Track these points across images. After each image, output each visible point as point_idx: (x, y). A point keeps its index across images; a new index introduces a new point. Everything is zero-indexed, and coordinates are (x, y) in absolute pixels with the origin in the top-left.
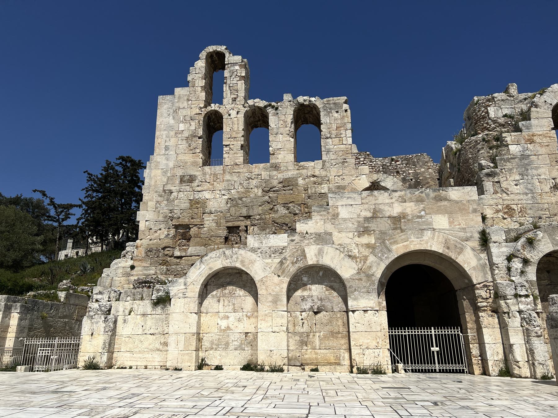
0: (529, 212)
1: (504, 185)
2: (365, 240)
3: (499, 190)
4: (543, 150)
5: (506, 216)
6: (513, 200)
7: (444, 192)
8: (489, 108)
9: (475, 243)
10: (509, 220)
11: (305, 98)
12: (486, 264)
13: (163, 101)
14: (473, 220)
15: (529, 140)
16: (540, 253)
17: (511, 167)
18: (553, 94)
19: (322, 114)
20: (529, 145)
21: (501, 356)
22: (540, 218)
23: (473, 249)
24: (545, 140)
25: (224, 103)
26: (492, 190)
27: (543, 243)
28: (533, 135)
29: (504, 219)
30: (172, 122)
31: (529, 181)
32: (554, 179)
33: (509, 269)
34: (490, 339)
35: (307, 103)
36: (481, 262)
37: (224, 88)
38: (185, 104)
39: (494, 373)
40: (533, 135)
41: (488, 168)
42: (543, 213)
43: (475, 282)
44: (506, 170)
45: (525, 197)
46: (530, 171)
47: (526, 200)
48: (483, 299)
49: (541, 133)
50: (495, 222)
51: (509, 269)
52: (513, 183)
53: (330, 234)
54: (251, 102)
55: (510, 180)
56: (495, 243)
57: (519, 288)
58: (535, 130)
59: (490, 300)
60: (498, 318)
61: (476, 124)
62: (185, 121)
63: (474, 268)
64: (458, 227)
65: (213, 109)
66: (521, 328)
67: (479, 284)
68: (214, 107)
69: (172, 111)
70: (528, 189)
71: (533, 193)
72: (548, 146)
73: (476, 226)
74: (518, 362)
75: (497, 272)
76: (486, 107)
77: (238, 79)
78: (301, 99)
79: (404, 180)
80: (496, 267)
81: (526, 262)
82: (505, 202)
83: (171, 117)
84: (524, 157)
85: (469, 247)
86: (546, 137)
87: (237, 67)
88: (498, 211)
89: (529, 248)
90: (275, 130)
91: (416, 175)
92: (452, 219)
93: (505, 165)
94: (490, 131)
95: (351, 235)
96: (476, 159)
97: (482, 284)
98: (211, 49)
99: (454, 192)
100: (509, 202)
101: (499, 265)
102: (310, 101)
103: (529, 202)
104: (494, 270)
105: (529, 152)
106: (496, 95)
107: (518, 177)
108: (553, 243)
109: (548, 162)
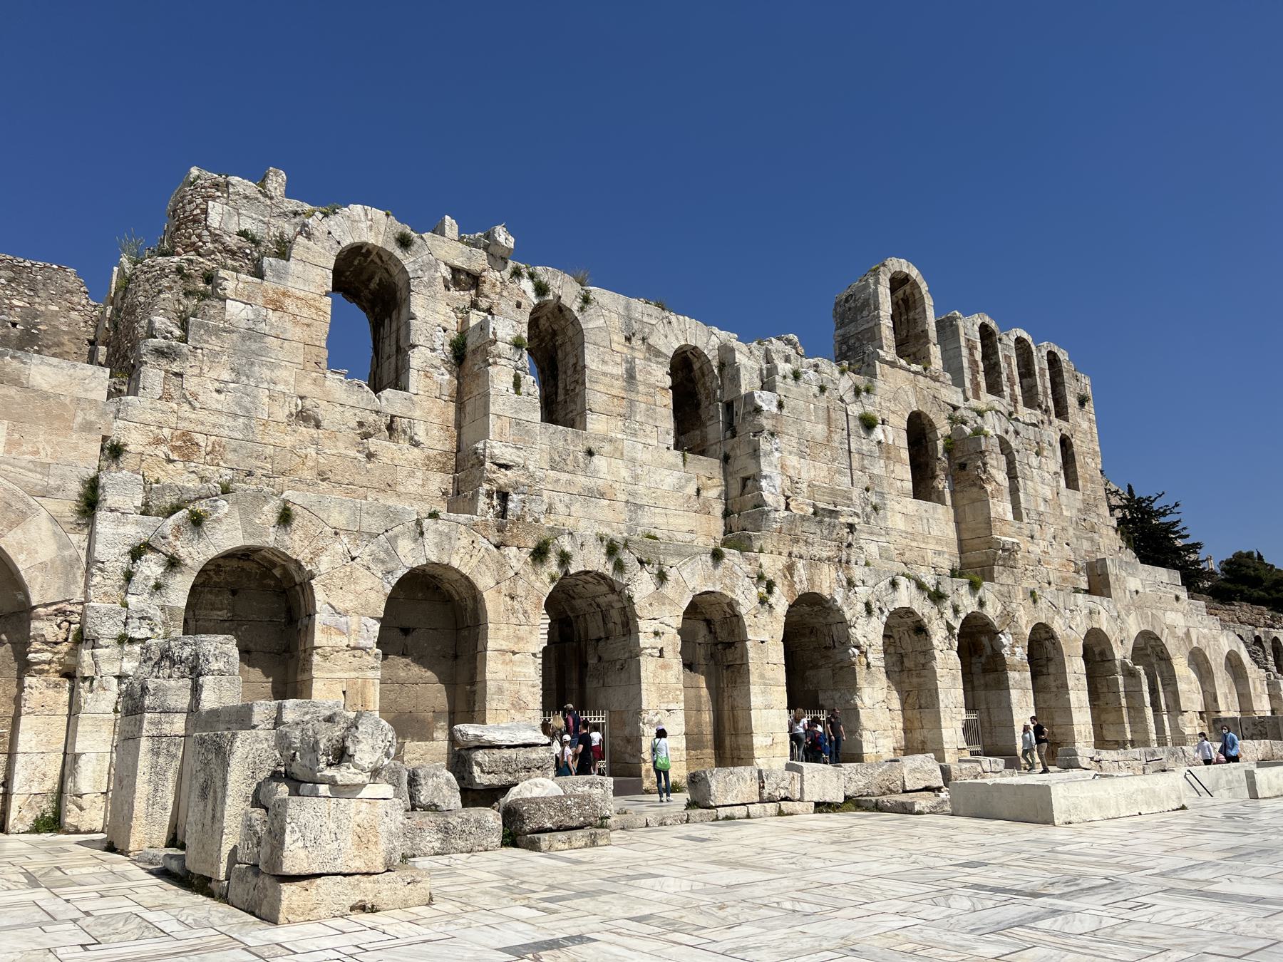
0: (230, 456)
1: (191, 384)
3: (176, 394)
4: (296, 332)
5: (174, 456)
6: (202, 424)
7: (15, 364)
8: (210, 203)
9: (67, 506)
10: (180, 465)
12: (78, 559)
14: (75, 448)
15: (273, 301)
16: (212, 548)
17: (218, 349)
18: (348, 223)
20: (270, 312)
21: (51, 784)
22: (250, 474)
23: (55, 520)
24: (306, 312)
26: (159, 391)
27: (224, 527)
28: (284, 294)
29: (170, 461)
31: (249, 389)
32: (302, 398)
33: (129, 576)
34: (33, 744)
36: (66, 553)
39: (20, 827)
40: (284, 294)
41: (165, 338)
42: (259, 464)
43: (35, 600)
44: (206, 351)
45: (231, 423)
46: (256, 368)
47: (231, 429)
48: (46, 643)
49: (302, 294)
50: (144, 464)
51: (129, 576)
52: (212, 386)
55: (207, 377)
56: (112, 511)
57: (134, 623)
58: (291, 285)
59: (64, 648)
60: (72, 690)
61: (178, 229)
63: (43, 566)
64: (29, 457)
66: (112, 716)
67: (46, 605)
70: (241, 406)
71: (250, 418)
72: (308, 325)
73: (81, 464)
74: (80, 796)
75: (96, 580)
76: (206, 198)
80: (100, 569)
81: (173, 564)
82: (182, 425)
84: (252, 334)
85: (44, 513)
86: (310, 306)
88: (158, 441)
89: (189, 535)
92: (17, 436)
93: (206, 342)
94: (199, 255)
96: (149, 308)
97: (54, 607)
99: (45, 369)
100: (191, 427)
101: (107, 565)
103: (236, 435)
104: (93, 575)
105: (267, 328)
106: (234, 179)
107: (226, 375)
108: (245, 531)
109: (301, 359)
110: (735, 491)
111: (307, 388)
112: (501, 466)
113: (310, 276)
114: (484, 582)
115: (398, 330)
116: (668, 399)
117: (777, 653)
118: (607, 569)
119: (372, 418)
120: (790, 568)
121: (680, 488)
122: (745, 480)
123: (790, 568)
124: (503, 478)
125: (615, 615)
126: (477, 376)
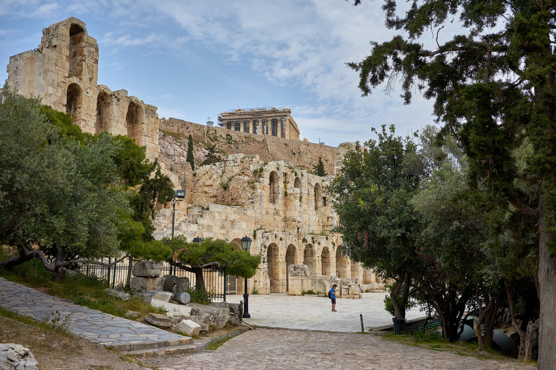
1: (255, 208)
2: (223, 231)
13: (36, 58)
19: (145, 115)
25: (83, 80)
30: (42, 82)
37: (84, 65)
38: (53, 68)
53: (212, 227)
62: (52, 85)
69: (43, 71)
76: (250, 164)
77: (94, 61)
79: (179, 178)
83: (42, 77)
90: (117, 118)
91: (185, 175)
110: (325, 220)
111: (268, 206)
113: (266, 180)
114: (297, 247)
115: (274, 188)
116: (314, 198)
117: (335, 259)
118: (311, 243)
119: (275, 211)
120: (337, 240)
121: (316, 220)
122: (328, 218)
123: (337, 240)
125: (309, 252)
126: (292, 201)
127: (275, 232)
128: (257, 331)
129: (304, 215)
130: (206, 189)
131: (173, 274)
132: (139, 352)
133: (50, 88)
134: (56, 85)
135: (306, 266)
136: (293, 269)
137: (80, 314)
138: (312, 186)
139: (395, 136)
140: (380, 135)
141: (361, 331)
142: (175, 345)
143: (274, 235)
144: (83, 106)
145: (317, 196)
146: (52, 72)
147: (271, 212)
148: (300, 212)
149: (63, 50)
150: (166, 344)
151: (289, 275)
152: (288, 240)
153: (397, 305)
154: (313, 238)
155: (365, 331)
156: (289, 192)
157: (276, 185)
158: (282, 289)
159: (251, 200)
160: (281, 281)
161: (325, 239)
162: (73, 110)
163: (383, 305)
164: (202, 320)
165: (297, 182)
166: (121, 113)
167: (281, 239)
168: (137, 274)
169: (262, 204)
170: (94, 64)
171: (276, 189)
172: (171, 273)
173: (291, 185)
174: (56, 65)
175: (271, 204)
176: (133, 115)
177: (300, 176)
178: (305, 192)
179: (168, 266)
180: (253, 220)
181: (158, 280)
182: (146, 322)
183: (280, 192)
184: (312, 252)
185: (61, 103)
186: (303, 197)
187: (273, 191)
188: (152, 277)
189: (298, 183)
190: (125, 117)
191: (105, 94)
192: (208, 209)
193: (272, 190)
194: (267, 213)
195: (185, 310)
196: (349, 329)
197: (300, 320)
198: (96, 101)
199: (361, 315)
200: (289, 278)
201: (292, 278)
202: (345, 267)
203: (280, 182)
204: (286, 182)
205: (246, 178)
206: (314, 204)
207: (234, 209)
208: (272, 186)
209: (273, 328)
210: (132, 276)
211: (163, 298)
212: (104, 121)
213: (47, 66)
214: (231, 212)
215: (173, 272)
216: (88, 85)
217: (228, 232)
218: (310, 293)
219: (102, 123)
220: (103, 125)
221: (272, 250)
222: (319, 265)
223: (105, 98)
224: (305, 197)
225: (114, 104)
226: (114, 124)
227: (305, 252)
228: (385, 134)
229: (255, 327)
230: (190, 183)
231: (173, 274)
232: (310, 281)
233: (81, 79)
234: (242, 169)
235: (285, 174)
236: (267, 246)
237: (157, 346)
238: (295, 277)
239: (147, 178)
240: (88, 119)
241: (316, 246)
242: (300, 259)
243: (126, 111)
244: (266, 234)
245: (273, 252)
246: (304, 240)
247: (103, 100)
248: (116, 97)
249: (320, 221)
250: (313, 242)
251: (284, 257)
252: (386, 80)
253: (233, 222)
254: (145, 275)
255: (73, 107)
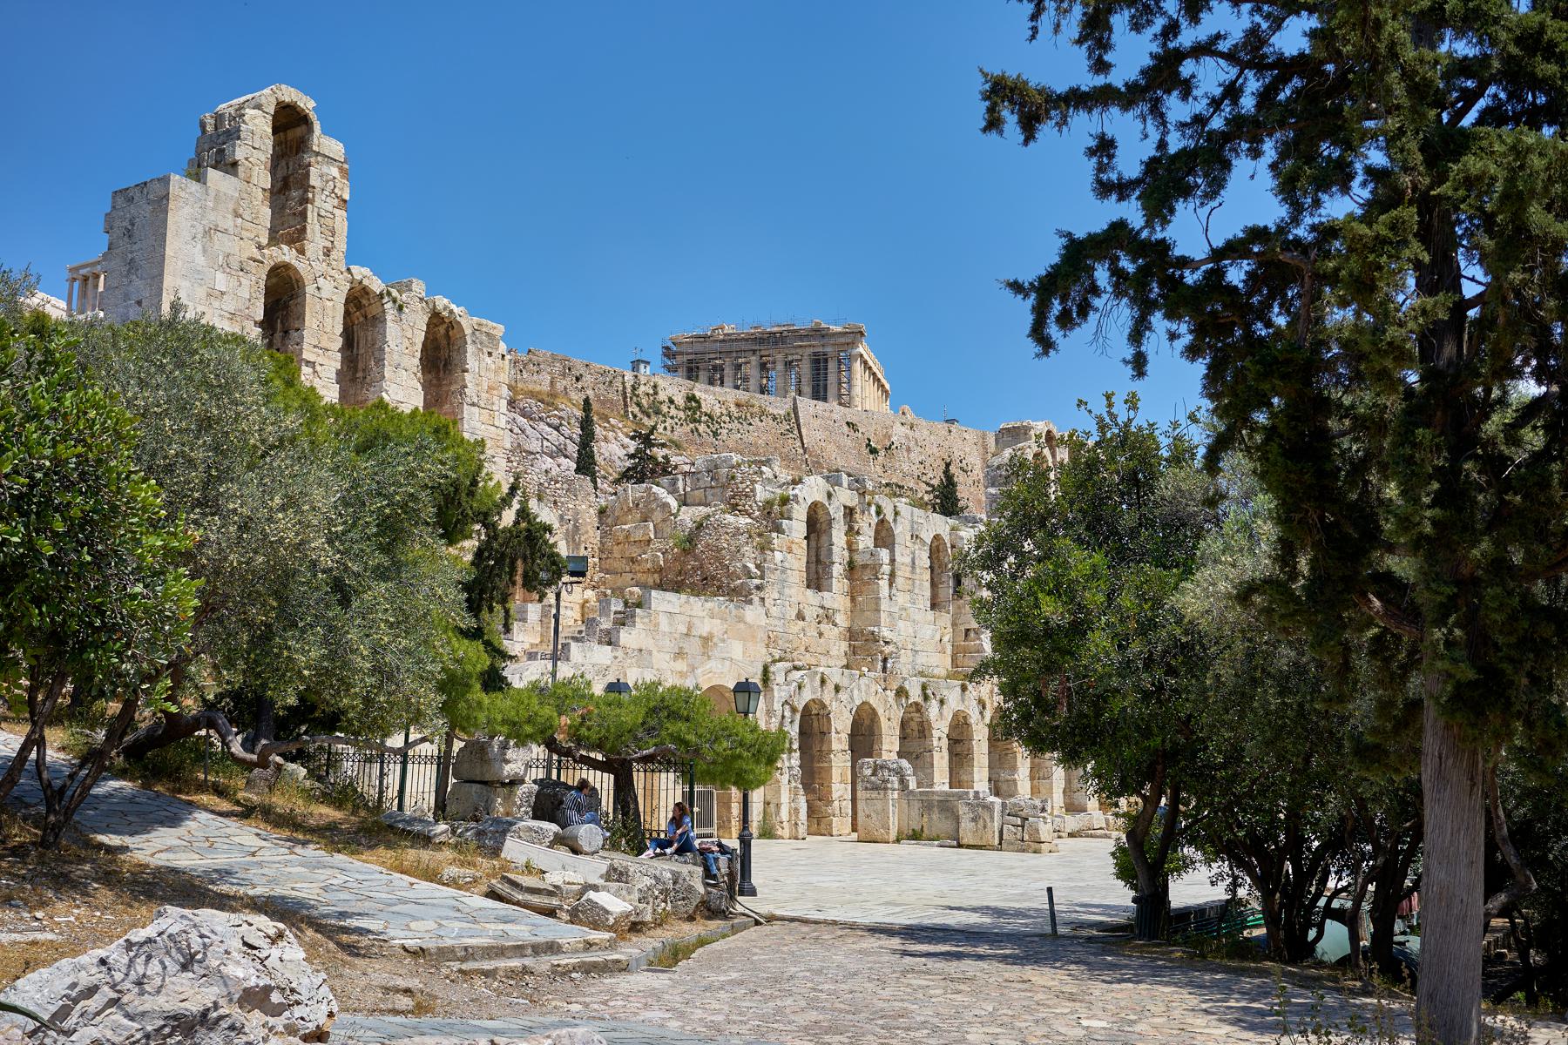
2: (681, 666)
11: (446, 301)
13: (182, 194)
19: (470, 348)
25: (308, 254)
30: (200, 260)
35: (445, 314)
38: (228, 222)
53: (650, 653)
54: (360, 272)
65: (287, 259)
68: (287, 254)
69: (201, 229)
76: (753, 482)
78: (442, 302)
83: (199, 246)
87: (335, 172)
90: (395, 357)
95: (667, 657)
98: (289, 94)
102: (451, 312)
112: (887, 643)
113: (797, 527)
114: (880, 711)
115: (818, 548)
121: (933, 637)
124: (887, 649)
125: (914, 725)
127: (821, 669)
128: (777, 926)
129: (901, 624)
130: (634, 551)
131: (554, 777)
132: (487, 965)
133: (220, 276)
134: (236, 266)
135: (905, 763)
136: (868, 772)
137: (329, 872)
138: (923, 542)
139: (1140, 420)
140: (1100, 420)
141: (1048, 929)
142: (576, 951)
143: (818, 678)
144: (307, 323)
145: (937, 570)
146: (225, 232)
147: (810, 613)
148: (891, 613)
149: (255, 174)
150: (552, 948)
151: (859, 787)
152: (856, 692)
153: (1145, 864)
154: (924, 688)
155: (1062, 930)
156: (859, 559)
157: (824, 538)
158: (841, 824)
159: (757, 582)
160: (836, 803)
161: (959, 689)
162: (278, 335)
163: (1110, 865)
164: (636, 896)
165: (884, 536)
166: (407, 343)
167: (837, 689)
168: (466, 776)
169: (787, 591)
170: (336, 211)
171: (823, 552)
172: (549, 773)
173: (865, 541)
174: (237, 215)
175: (809, 592)
176: (437, 348)
177: (890, 517)
178: (902, 558)
179: (541, 756)
180: (761, 635)
181: (522, 790)
182: (493, 895)
183: (836, 558)
184: (921, 724)
185: (248, 317)
186: (898, 573)
187: (817, 556)
188: (503, 785)
189: (884, 533)
190: (418, 355)
191: (365, 291)
192: (639, 605)
193: (813, 553)
194: (801, 616)
195: (590, 869)
196: (1017, 925)
197: (887, 903)
198: (341, 310)
199: (1050, 890)
200: (859, 794)
201: (868, 794)
202: (1014, 769)
203: (834, 532)
204: (851, 531)
205: (743, 521)
206: (928, 594)
207: (709, 605)
208: (813, 544)
209: (816, 922)
210: (452, 780)
211: (536, 837)
212: (361, 365)
213: (212, 216)
214: (701, 612)
215: (554, 772)
216: (320, 267)
217: (693, 669)
218: (916, 836)
219: (356, 371)
220: (360, 374)
221: (813, 724)
222: (941, 761)
223: (364, 302)
224: (903, 573)
225: (389, 317)
226: (388, 372)
227: (903, 725)
228: (1113, 416)
229: (771, 919)
230: (591, 533)
231: (554, 777)
232: (917, 805)
233: (302, 252)
234: (733, 497)
235: (849, 512)
236: (800, 708)
237: (529, 951)
238: (874, 794)
239: (494, 525)
240: (320, 360)
241: (933, 710)
242: (890, 744)
243: (420, 338)
244: (797, 675)
245: (815, 724)
246: (901, 692)
247: (359, 307)
248: (395, 301)
249: (946, 639)
250: (926, 698)
251: (844, 737)
252: (1093, 317)
253: (706, 640)
254: (487, 778)
255: (279, 325)
